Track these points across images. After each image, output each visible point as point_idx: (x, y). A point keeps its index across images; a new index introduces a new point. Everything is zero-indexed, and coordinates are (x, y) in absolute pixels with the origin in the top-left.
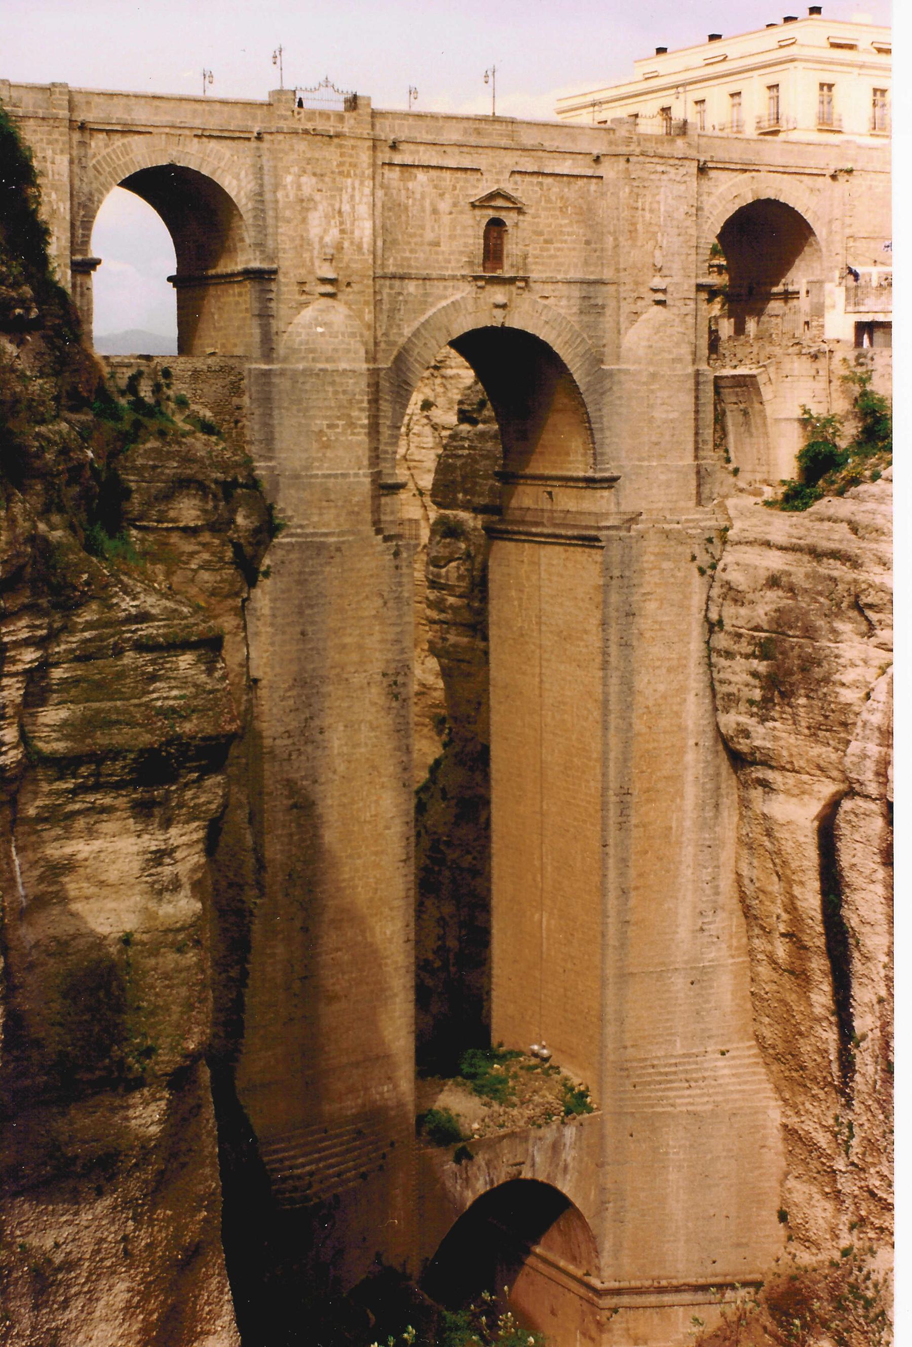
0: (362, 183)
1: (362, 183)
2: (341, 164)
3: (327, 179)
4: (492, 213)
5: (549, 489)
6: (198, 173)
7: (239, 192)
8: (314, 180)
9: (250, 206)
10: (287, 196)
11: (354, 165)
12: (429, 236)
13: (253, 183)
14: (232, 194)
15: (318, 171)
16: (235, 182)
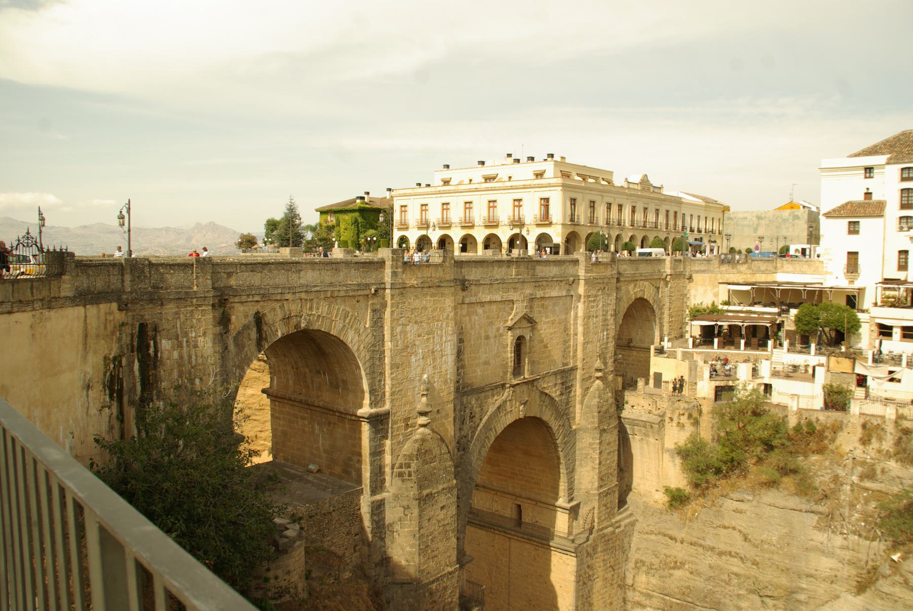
0: (447, 326)
1: (447, 326)
2: (434, 310)
3: (425, 325)
4: (518, 333)
5: (519, 503)
6: (327, 334)
7: (359, 346)
8: (416, 327)
9: (368, 358)
10: (397, 346)
11: (443, 310)
12: (483, 357)
13: (370, 336)
14: (354, 349)
15: (418, 319)
16: (356, 338)
